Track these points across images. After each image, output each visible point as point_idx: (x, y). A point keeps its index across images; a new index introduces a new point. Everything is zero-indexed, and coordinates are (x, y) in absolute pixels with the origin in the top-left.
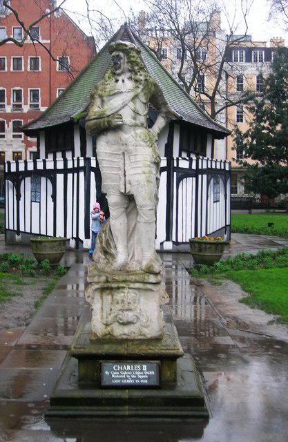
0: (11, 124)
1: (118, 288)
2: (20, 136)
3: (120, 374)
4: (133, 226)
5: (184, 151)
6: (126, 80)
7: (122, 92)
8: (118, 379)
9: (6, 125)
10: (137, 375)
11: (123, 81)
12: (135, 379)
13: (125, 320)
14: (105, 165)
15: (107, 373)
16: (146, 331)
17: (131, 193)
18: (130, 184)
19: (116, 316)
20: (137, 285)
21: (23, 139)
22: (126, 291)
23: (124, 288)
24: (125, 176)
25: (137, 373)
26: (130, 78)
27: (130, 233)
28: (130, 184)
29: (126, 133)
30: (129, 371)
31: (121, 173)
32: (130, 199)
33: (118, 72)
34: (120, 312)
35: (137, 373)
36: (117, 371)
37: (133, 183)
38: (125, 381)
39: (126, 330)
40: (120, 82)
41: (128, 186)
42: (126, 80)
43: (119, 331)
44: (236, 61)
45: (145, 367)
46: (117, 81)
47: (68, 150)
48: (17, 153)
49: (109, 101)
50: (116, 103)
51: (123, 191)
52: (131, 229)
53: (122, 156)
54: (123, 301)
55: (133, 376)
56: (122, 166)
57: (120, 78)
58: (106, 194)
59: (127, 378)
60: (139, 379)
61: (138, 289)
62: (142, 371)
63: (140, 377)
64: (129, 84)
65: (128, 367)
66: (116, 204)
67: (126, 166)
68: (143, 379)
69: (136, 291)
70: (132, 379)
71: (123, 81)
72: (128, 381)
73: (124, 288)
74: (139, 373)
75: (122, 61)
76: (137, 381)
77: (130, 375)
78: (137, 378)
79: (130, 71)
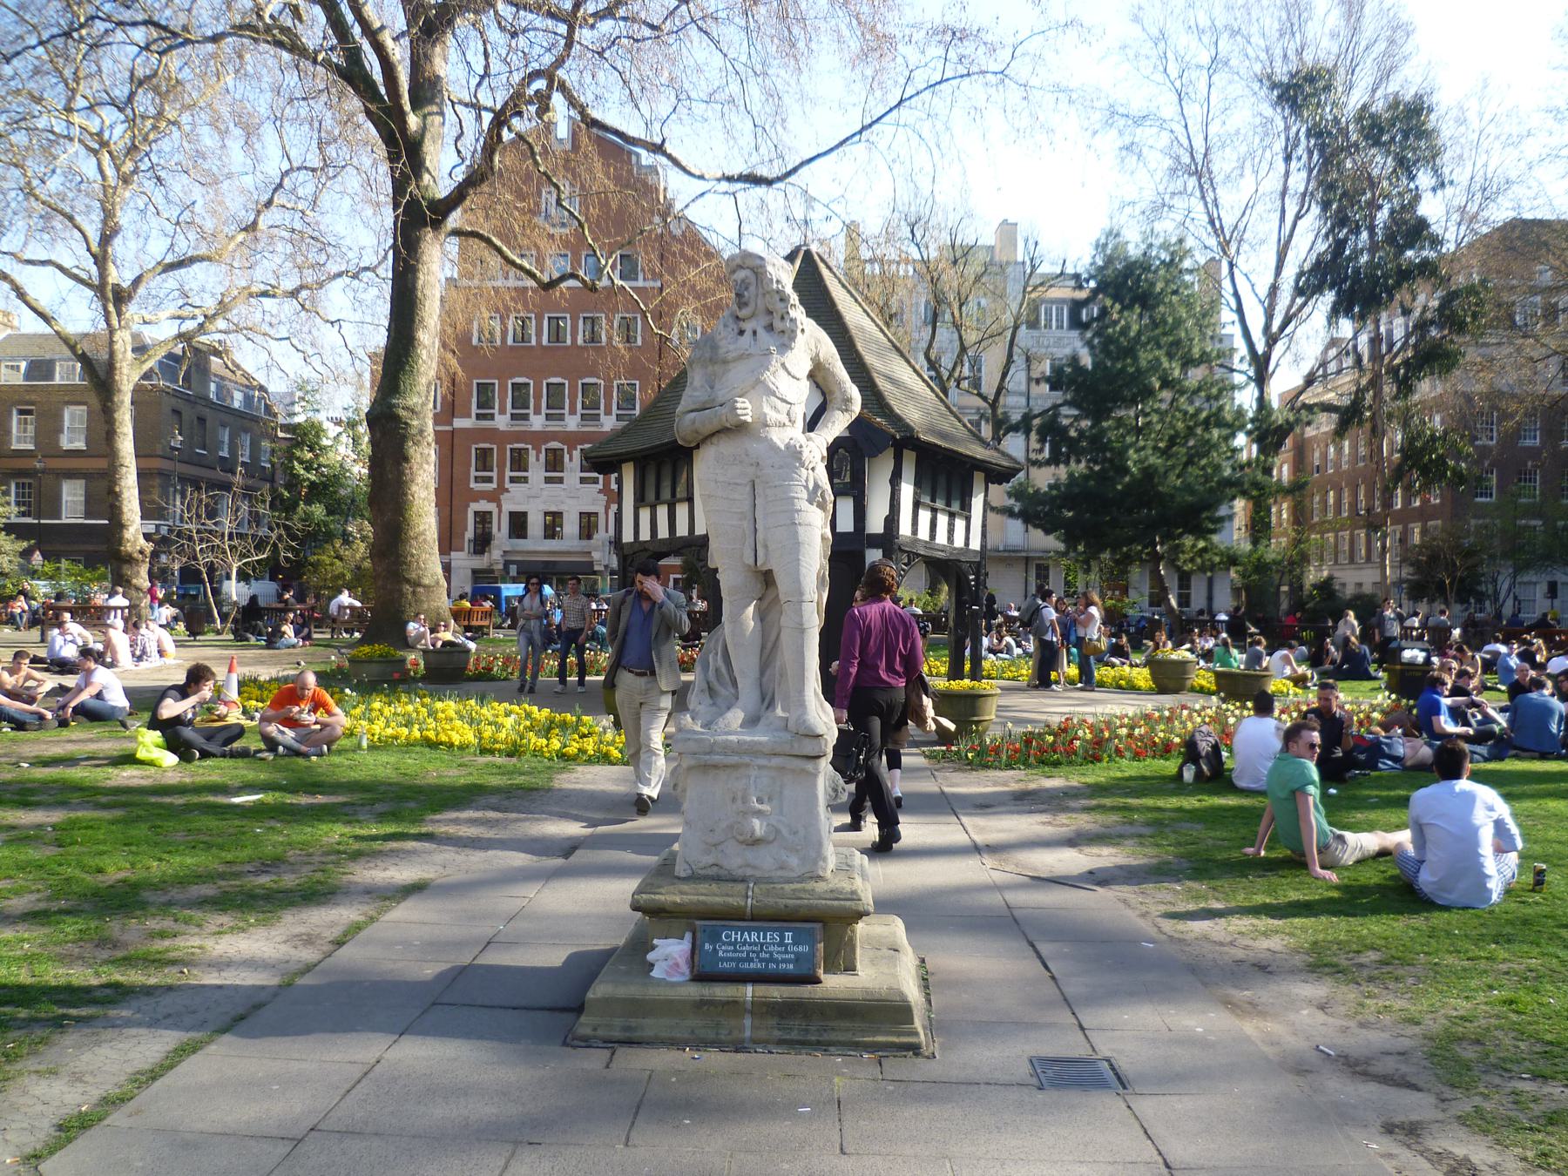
0: (576, 454)
1: (735, 767)
2: (595, 481)
3: (735, 951)
4: (773, 638)
5: (926, 506)
6: (761, 332)
8: (731, 959)
9: (567, 457)
10: (771, 953)
11: (755, 333)
12: (767, 961)
15: (707, 946)
19: (731, 827)
20: (776, 761)
21: (600, 486)
22: (754, 773)
23: (747, 765)
25: (771, 948)
27: (767, 651)
28: (766, 547)
30: (755, 944)
35: (771, 948)
36: (730, 944)
38: (746, 966)
39: (750, 855)
40: (748, 334)
42: (761, 332)
43: (735, 860)
44: (1048, 325)
45: (788, 934)
46: (741, 332)
47: (681, 501)
48: (589, 514)
51: (751, 561)
52: (769, 645)
53: (748, 488)
55: (763, 955)
57: (748, 326)
58: (716, 570)
59: (752, 960)
60: (777, 962)
61: (781, 769)
62: (781, 944)
63: (780, 957)
65: (754, 936)
68: (784, 961)
70: (761, 960)
71: (755, 333)
72: (752, 966)
73: (747, 765)
74: (776, 948)
76: (772, 966)
77: (757, 953)
78: (772, 960)
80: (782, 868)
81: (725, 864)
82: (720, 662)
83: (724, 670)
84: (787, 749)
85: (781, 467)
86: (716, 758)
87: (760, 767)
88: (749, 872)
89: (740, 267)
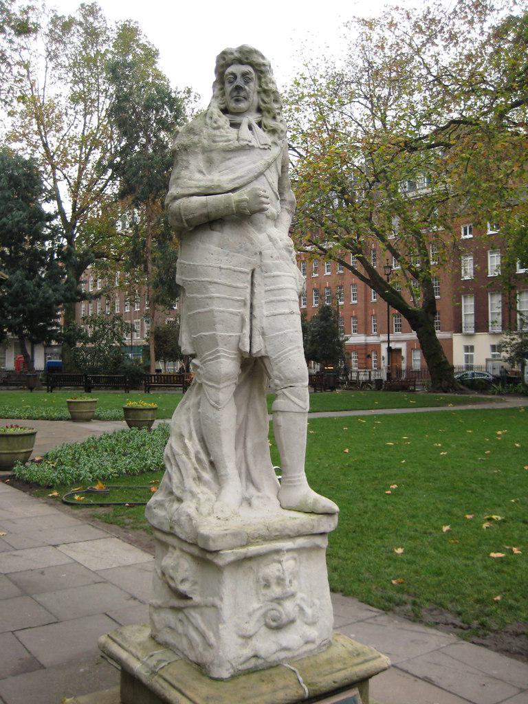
7: (253, 147)
11: (250, 128)
13: (285, 619)
14: (218, 295)
16: (313, 633)
17: (263, 353)
18: (263, 334)
19: (265, 615)
20: (301, 542)
22: (285, 557)
23: (278, 552)
24: (252, 316)
26: (260, 124)
28: (263, 334)
29: (260, 230)
31: (247, 312)
32: (254, 369)
33: (243, 105)
34: (275, 605)
37: (270, 334)
40: (244, 127)
41: (258, 339)
43: (267, 645)
49: (222, 162)
50: (244, 166)
51: (248, 349)
53: (249, 277)
54: (280, 581)
56: (248, 297)
61: (299, 550)
64: (263, 137)
66: (228, 377)
67: (257, 296)
69: (295, 555)
75: (252, 84)
79: (259, 110)
80: (307, 643)
81: (262, 653)
82: (199, 447)
83: (203, 456)
84: (308, 529)
85: (278, 258)
86: (253, 549)
87: (289, 550)
88: (283, 655)
89: (240, 62)
